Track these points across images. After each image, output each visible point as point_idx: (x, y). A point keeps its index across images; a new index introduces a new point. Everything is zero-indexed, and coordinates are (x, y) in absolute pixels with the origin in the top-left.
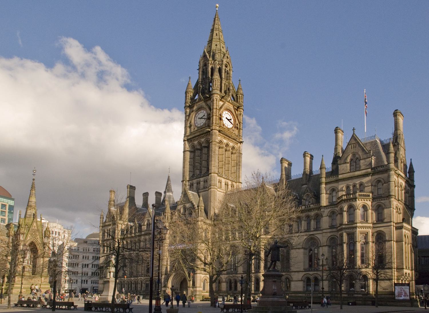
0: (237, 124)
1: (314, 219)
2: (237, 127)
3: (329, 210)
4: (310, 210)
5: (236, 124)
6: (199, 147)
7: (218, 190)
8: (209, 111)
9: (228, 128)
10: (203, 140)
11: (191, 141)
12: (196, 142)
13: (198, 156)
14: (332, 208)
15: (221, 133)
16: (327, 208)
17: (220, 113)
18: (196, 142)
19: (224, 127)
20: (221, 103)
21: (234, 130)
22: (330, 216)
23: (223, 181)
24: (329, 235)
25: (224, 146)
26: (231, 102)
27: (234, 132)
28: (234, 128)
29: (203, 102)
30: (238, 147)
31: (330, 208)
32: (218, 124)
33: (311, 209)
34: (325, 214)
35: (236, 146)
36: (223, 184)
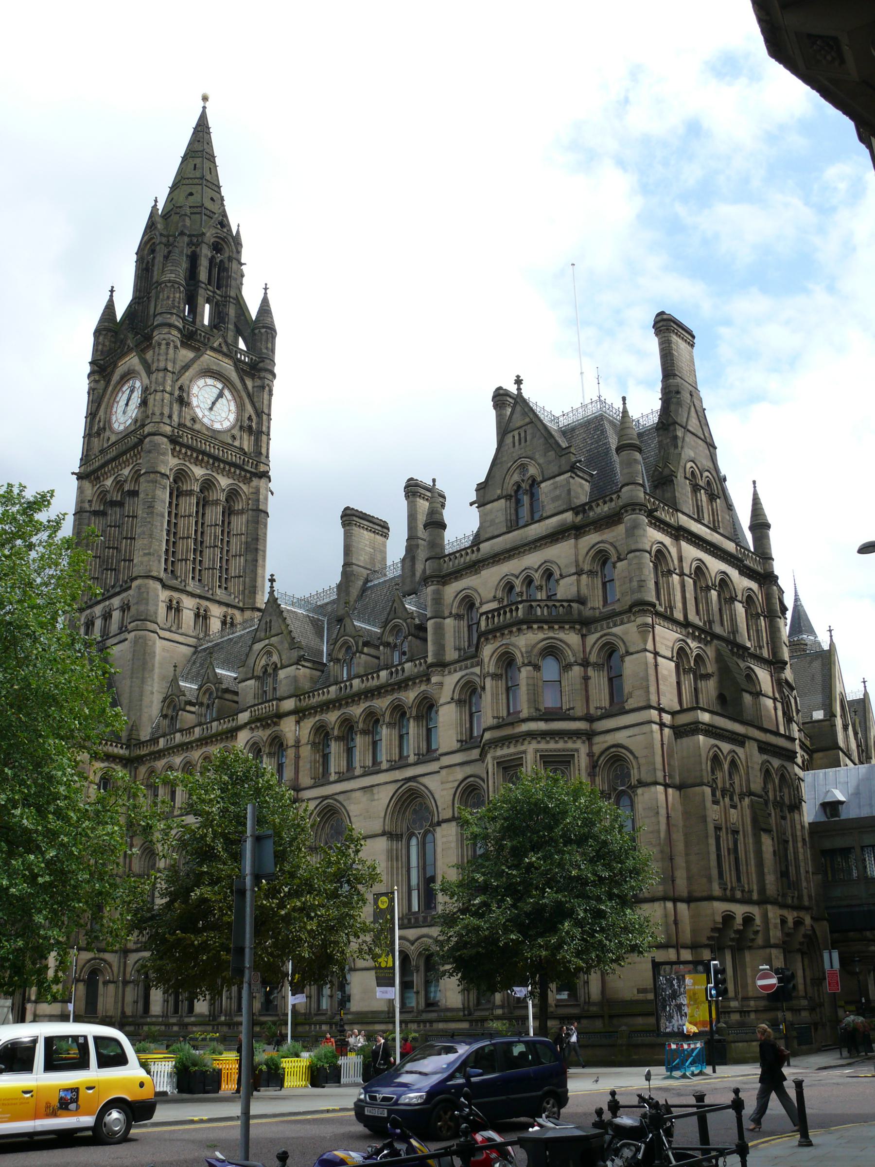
0: (250, 418)
1: (418, 718)
2: (250, 427)
3: (457, 676)
4: (403, 685)
5: (247, 416)
6: (117, 497)
7: (163, 634)
8: (146, 381)
9: (214, 431)
10: (126, 472)
11: (98, 478)
12: (109, 482)
13: (115, 526)
14: (466, 668)
15: (182, 445)
16: (450, 672)
17: (179, 383)
18: (109, 482)
19: (197, 427)
20: (186, 354)
21: (238, 438)
22: (460, 702)
23: (188, 603)
24: (459, 774)
25: (196, 488)
26: (225, 349)
27: (237, 444)
28: (236, 432)
29: (135, 354)
30: (251, 490)
31: (461, 669)
32: (170, 417)
33: (408, 679)
34: (445, 695)
35: (245, 488)
36: (188, 616)
